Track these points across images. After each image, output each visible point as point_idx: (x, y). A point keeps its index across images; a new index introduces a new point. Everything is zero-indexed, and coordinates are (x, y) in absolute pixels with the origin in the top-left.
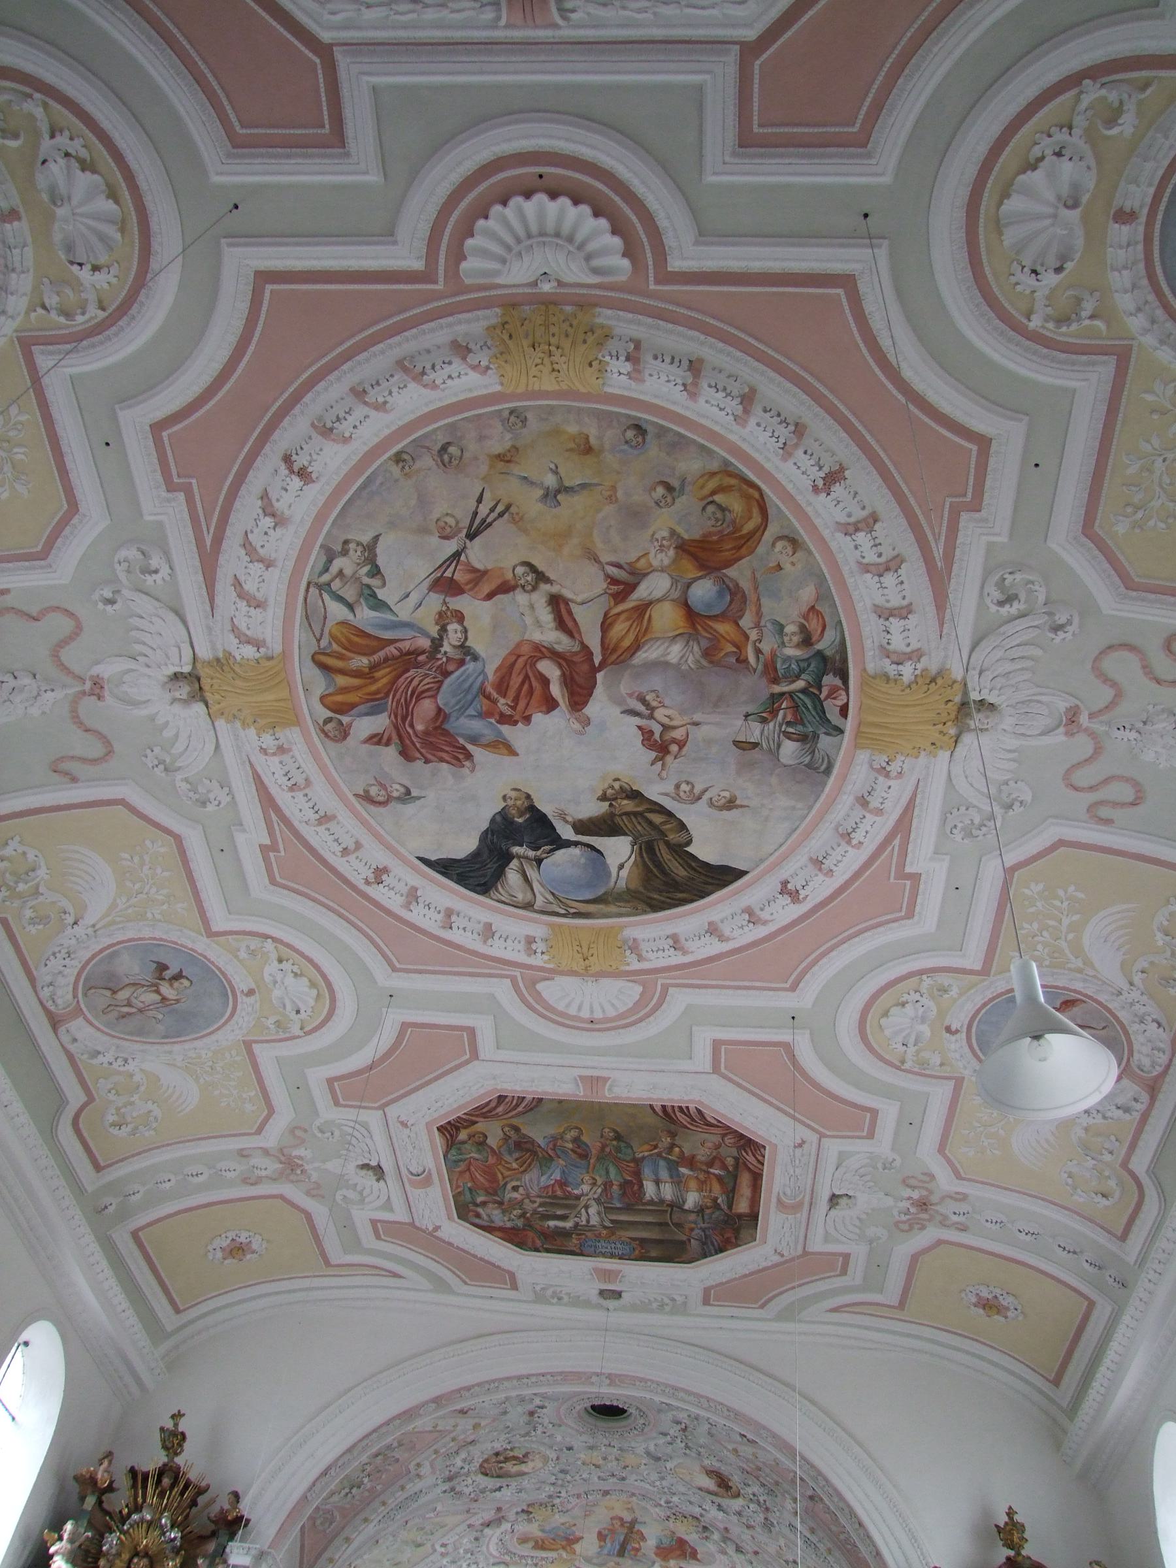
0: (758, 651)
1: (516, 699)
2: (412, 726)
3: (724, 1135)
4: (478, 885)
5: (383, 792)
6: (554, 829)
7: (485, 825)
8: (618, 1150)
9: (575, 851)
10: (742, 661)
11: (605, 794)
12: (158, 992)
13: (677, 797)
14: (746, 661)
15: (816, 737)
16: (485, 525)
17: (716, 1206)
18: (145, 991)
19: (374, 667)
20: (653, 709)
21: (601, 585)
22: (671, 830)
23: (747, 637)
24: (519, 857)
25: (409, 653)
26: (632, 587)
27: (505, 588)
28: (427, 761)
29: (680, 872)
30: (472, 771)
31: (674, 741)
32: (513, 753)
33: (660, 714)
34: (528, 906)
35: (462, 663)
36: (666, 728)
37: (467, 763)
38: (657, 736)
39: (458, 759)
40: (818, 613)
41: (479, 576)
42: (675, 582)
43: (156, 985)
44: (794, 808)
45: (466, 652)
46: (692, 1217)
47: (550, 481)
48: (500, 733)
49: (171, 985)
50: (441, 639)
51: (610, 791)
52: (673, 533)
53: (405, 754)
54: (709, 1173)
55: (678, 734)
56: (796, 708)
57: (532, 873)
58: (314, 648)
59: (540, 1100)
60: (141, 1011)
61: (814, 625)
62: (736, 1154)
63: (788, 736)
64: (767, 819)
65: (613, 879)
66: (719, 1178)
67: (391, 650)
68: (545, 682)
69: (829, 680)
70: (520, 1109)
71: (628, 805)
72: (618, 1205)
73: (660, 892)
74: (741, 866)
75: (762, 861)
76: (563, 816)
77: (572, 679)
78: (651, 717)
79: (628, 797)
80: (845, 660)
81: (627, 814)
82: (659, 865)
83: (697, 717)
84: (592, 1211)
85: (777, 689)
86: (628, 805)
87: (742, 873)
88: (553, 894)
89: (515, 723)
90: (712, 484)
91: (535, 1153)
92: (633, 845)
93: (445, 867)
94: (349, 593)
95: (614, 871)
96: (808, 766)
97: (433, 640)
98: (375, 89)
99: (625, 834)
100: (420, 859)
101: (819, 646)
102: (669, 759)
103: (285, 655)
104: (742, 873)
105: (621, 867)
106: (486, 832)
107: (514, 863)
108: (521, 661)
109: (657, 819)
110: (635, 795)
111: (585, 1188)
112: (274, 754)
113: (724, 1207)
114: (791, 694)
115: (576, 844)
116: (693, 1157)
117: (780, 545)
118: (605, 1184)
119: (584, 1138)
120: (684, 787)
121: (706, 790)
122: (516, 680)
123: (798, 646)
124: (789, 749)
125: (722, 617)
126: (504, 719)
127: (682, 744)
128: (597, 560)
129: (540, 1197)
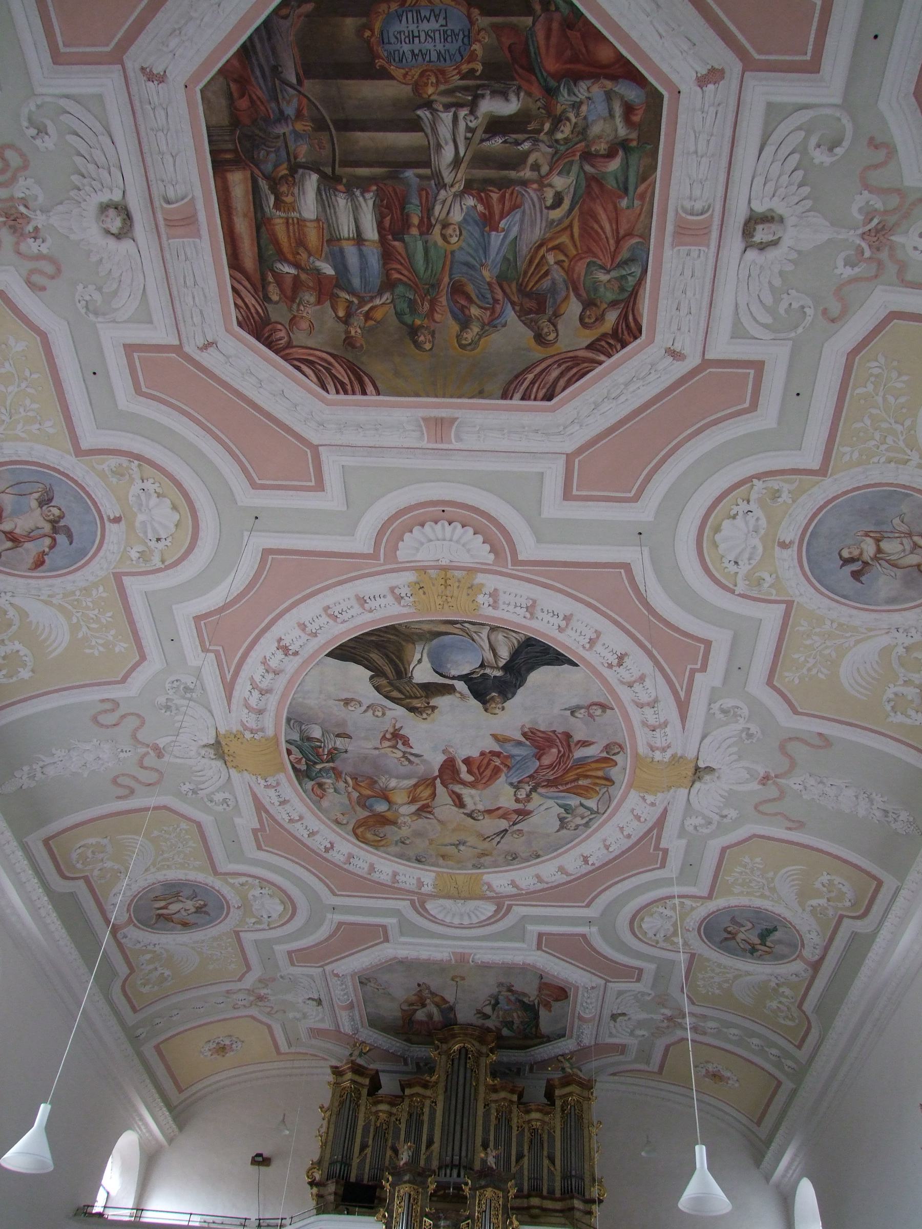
0: (346, 782)
1: (488, 764)
2: (559, 751)
3: (289, 345)
4: (533, 645)
5: (591, 711)
6: (469, 688)
7: (521, 691)
8: (412, 304)
9: (454, 672)
10: (354, 779)
11: (433, 711)
12: (879, 550)
13: (383, 707)
14: (352, 779)
15: (302, 739)
16: (498, 834)
17: (274, 184)
18: (889, 555)
19: (577, 780)
20: (403, 757)
21: (436, 811)
22: (385, 687)
23: (354, 788)
24: (498, 668)
25: (552, 786)
26: (418, 809)
27: (489, 812)
28: (554, 732)
29: (375, 656)
30: (523, 726)
31: (389, 740)
32: (492, 735)
33: (400, 754)
34: (493, 629)
35: (519, 782)
36: (395, 747)
37: (526, 730)
38: (400, 742)
39: (532, 732)
40: (317, 796)
41: (504, 816)
42: (397, 811)
43: (876, 558)
44: (304, 698)
45: (517, 787)
46: (303, 151)
47: (462, 848)
48: (501, 747)
49: (861, 554)
50: (530, 792)
51: (429, 712)
52: (400, 828)
53: (568, 736)
54: (297, 266)
55: (387, 744)
56: (318, 755)
57: (489, 656)
58: (611, 789)
59: (504, 396)
60: (910, 535)
61: (319, 792)
62: (270, 307)
63: (318, 740)
64: (321, 692)
65: (425, 651)
66: (284, 259)
67: (561, 788)
68: (470, 772)
69: (303, 767)
70: (530, 377)
71: (417, 703)
72: (409, 173)
73: (389, 641)
74: (330, 660)
75: (317, 664)
76: (463, 696)
77: (453, 772)
78: (404, 753)
79: (417, 708)
80: (297, 776)
81: (417, 698)
82: (391, 661)
83: (377, 752)
84: (448, 153)
85: (331, 765)
86: (417, 703)
87: (329, 655)
88: (473, 640)
89: (490, 752)
90: (383, 843)
91: (521, 290)
92: (411, 677)
93: (558, 659)
94: (581, 810)
95: (425, 659)
96: (301, 724)
97: (536, 791)
98: (524, 941)
99: (417, 684)
100: (577, 665)
101: (313, 783)
102: (391, 730)
103: (631, 786)
104: (329, 655)
105: (420, 661)
106: (520, 686)
107: (502, 663)
108: (484, 781)
109: (395, 694)
110: (412, 709)
111: (457, 216)
112: (657, 749)
113: (263, 184)
114: (322, 762)
115: (454, 678)
116: (319, 302)
117: (345, 822)
118: (430, 226)
119: (455, 327)
120: (380, 714)
121: (365, 711)
122: (488, 773)
123: (325, 783)
124: (316, 733)
125: (369, 797)
126: (498, 754)
127: (384, 738)
128: (439, 821)
129: (525, 183)
